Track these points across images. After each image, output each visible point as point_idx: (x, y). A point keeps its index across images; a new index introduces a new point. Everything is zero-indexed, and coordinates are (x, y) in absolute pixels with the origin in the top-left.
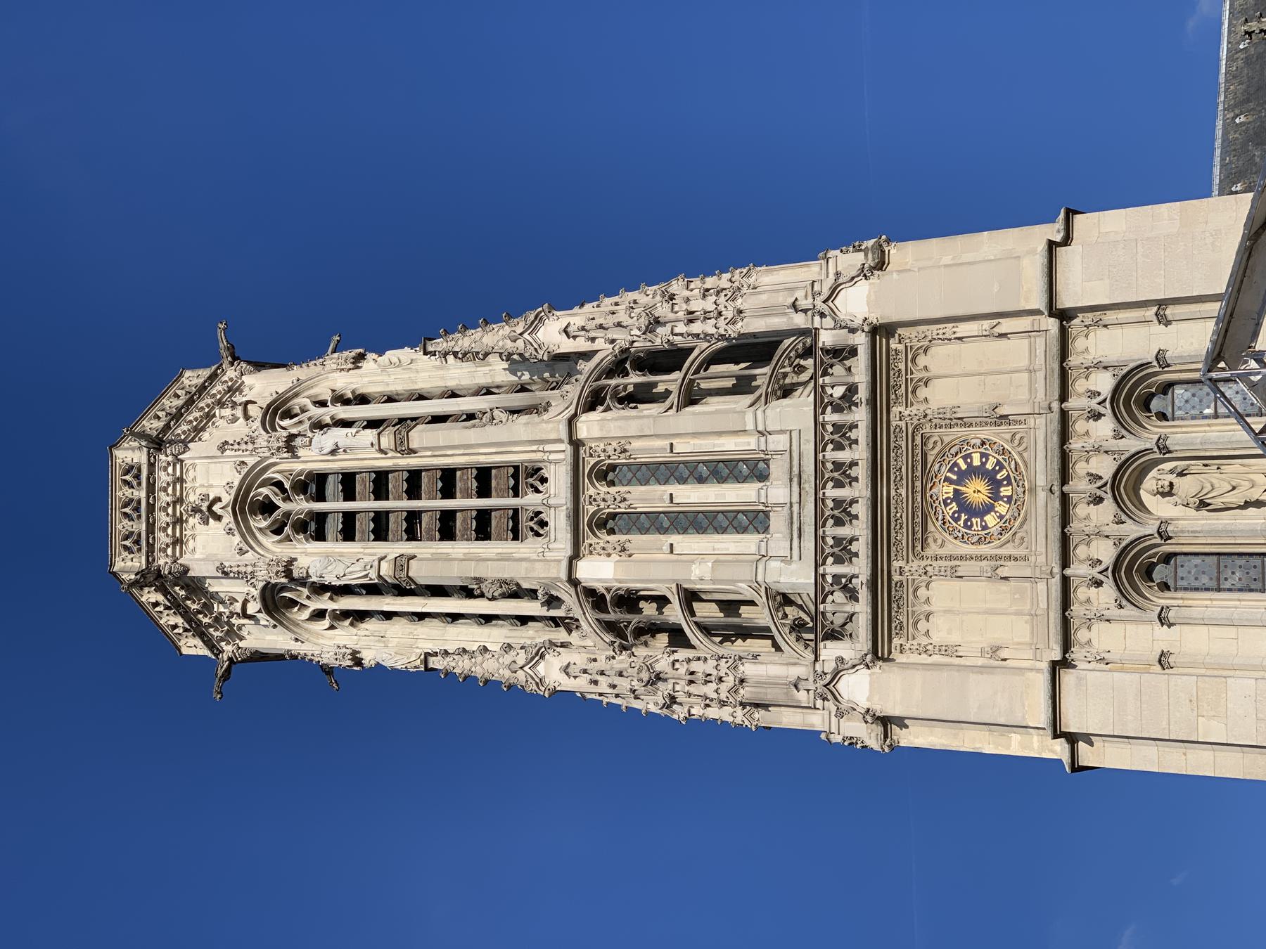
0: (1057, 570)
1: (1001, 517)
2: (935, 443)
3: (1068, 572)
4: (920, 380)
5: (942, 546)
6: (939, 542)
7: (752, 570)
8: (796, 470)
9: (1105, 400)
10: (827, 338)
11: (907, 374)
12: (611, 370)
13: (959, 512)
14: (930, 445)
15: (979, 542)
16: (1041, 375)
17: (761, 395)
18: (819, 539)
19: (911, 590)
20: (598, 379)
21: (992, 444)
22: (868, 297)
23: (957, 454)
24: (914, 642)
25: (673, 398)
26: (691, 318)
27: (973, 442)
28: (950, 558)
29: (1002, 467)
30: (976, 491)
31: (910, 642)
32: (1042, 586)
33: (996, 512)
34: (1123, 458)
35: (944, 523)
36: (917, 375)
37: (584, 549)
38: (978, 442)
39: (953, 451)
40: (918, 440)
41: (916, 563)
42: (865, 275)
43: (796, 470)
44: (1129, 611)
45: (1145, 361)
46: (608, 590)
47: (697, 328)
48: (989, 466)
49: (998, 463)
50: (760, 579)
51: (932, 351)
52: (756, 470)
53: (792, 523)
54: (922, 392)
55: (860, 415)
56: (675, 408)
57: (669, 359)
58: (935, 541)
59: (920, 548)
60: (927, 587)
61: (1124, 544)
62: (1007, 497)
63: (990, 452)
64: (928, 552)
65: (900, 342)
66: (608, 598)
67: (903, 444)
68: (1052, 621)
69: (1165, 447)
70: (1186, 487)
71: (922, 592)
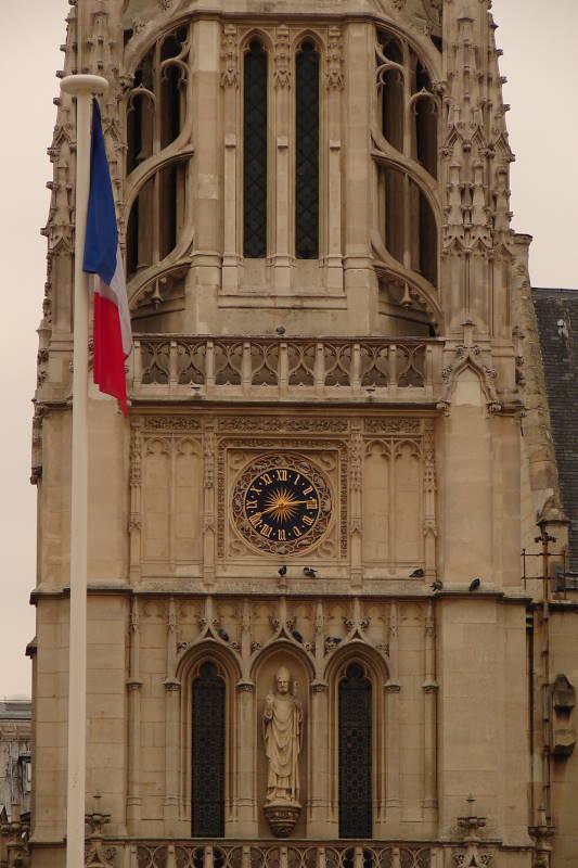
0: (213, 591)
1: (258, 529)
2: (328, 464)
3: (209, 602)
4: (388, 451)
5: (231, 469)
6: (236, 467)
7: (208, 249)
8: (307, 304)
9: (360, 638)
10: (433, 353)
11: (395, 436)
12: (421, 67)
13: (263, 487)
14: (326, 460)
15: (236, 507)
16: (384, 573)
17: (383, 261)
18: (238, 341)
19: (191, 437)
20: (412, 52)
21: (325, 522)
22: (470, 406)
23: (317, 485)
24: (142, 440)
25: (388, 151)
26: (466, 192)
27: (328, 502)
28: (221, 480)
29: (303, 531)
30: (282, 503)
31: (142, 436)
32: (194, 571)
33: (262, 524)
34: (309, 653)
35: (253, 471)
36: (392, 448)
37: (231, 28)
38: (327, 508)
39: (321, 482)
40: (334, 448)
41: (216, 443)
42: (490, 405)
43: (307, 304)
44: (174, 658)
45: (391, 673)
46: (186, 59)
47: (455, 199)
48: (305, 518)
49: (308, 527)
50: (201, 260)
51: (415, 463)
52: (307, 245)
53: (255, 297)
54: (376, 453)
55: (355, 392)
56: (377, 152)
57: (426, 153)
58: (237, 462)
59: (230, 446)
60: (193, 454)
61: (234, 651)
62: (271, 477)
63: (318, 519)
64: (226, 455)
65: (427, 431)
66: (177, 59)
67: (329, 432)
68: (162, 582)
69: (316, 691)
70: (282, 709)
71: (188, 449)
